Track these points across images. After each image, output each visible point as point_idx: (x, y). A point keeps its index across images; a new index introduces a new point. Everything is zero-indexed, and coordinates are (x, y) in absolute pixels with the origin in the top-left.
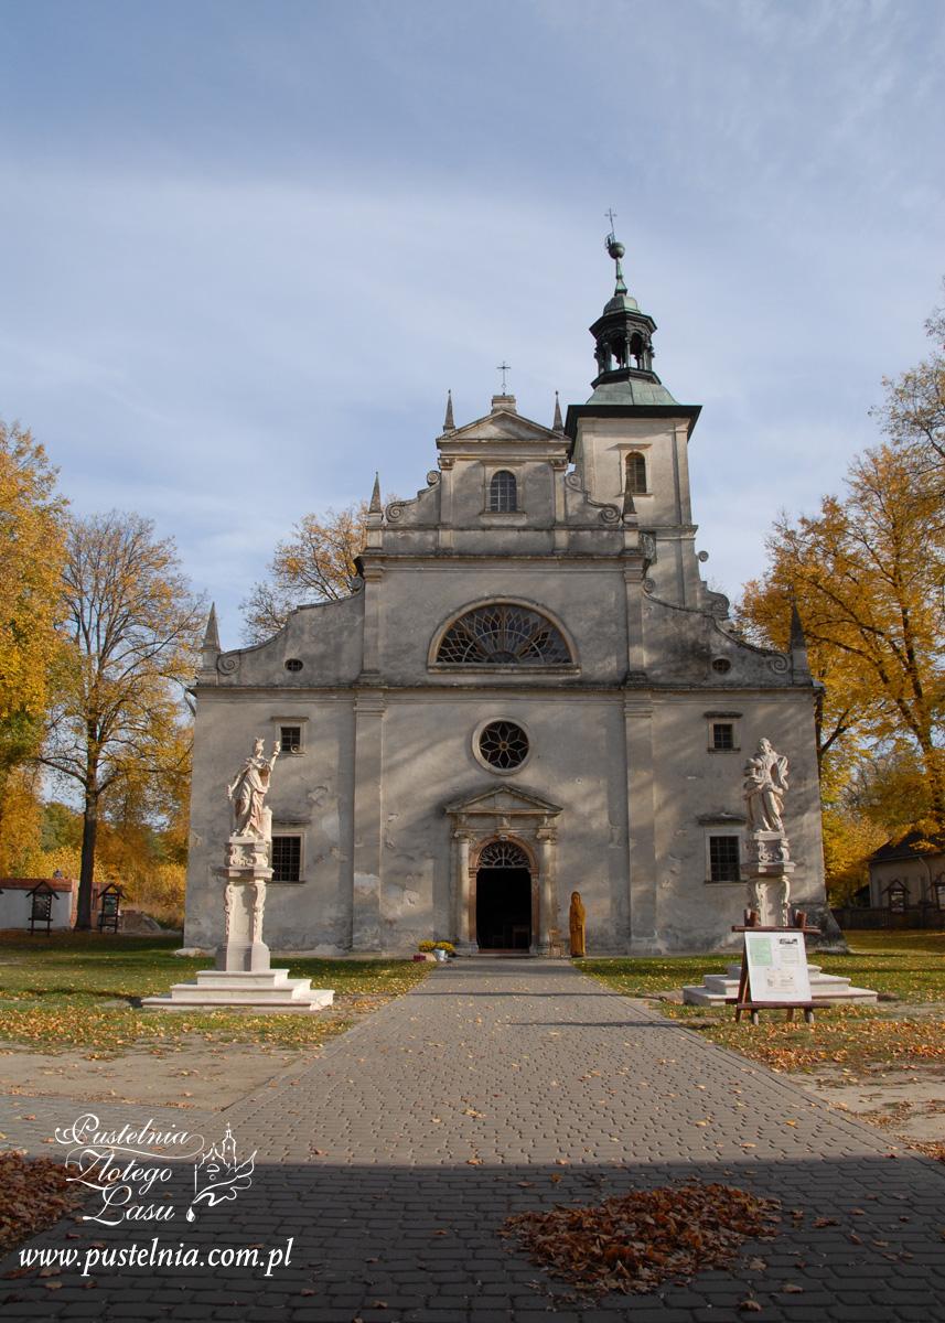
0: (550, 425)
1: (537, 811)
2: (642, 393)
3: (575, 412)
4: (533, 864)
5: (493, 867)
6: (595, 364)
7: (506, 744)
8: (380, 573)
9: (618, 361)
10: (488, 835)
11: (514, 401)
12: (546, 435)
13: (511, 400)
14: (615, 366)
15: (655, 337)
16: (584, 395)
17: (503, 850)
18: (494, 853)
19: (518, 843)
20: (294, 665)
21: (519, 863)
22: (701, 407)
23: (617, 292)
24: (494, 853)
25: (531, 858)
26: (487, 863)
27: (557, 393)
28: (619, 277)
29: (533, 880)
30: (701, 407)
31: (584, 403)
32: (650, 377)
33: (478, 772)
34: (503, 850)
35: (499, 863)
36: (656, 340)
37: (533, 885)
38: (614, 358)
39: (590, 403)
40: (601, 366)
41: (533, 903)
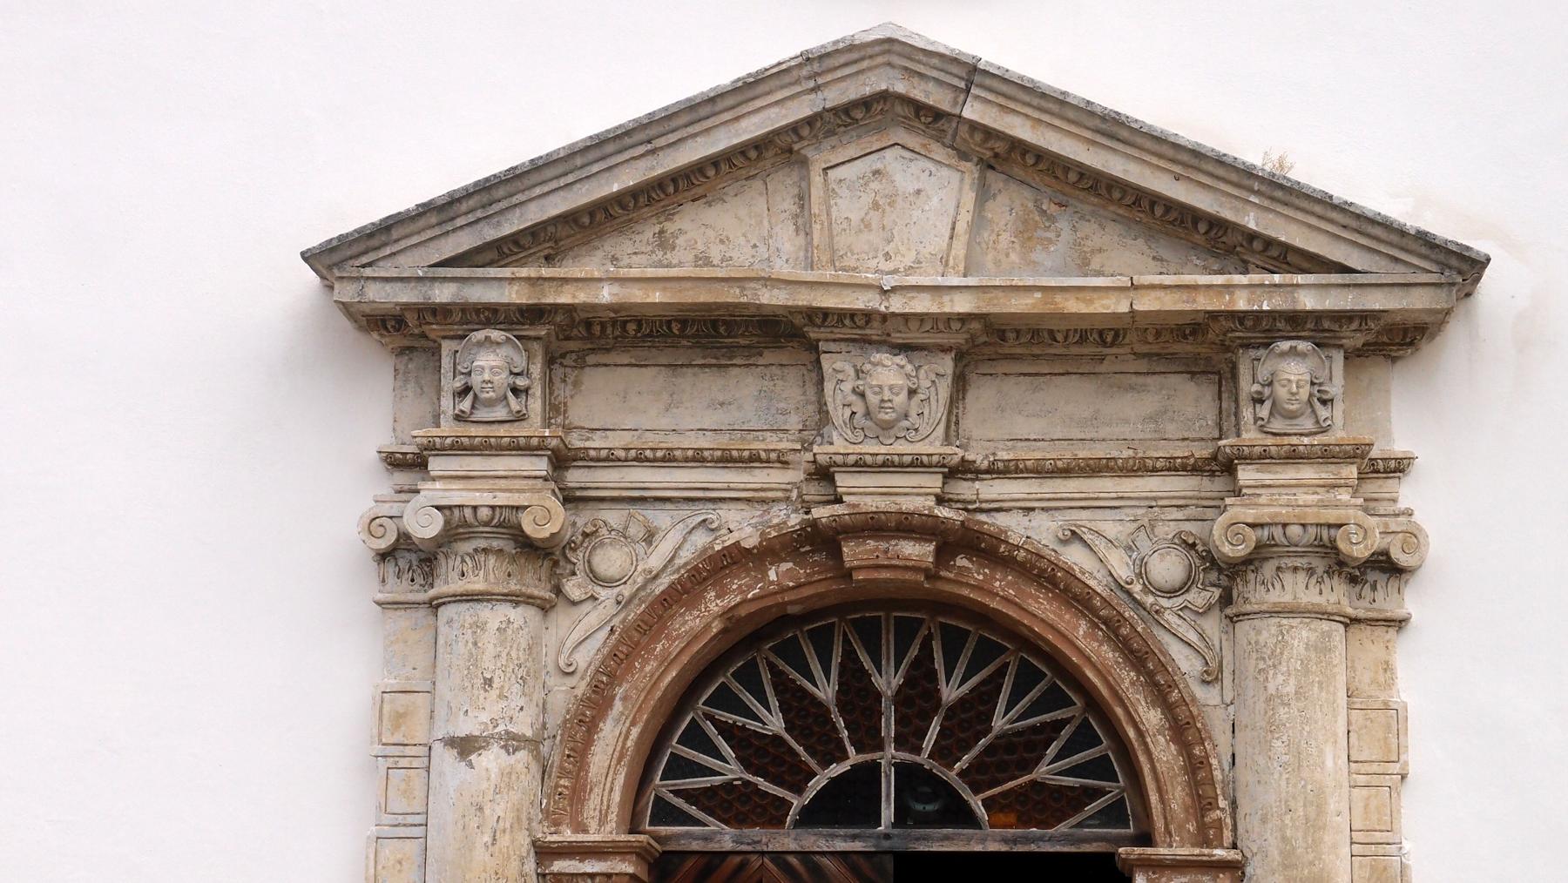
1: (1248, 291)
4: (1169, 796)
5: (787, 840)
10: (743, 528)
17: (888, 682)
18: (800, 708)
19: (1040, 610)
21: (1046, 805)
24: (800, 708)
25: (1163, 753)
26: (731, 804)
34: (888, 682)
35: (849, 802)
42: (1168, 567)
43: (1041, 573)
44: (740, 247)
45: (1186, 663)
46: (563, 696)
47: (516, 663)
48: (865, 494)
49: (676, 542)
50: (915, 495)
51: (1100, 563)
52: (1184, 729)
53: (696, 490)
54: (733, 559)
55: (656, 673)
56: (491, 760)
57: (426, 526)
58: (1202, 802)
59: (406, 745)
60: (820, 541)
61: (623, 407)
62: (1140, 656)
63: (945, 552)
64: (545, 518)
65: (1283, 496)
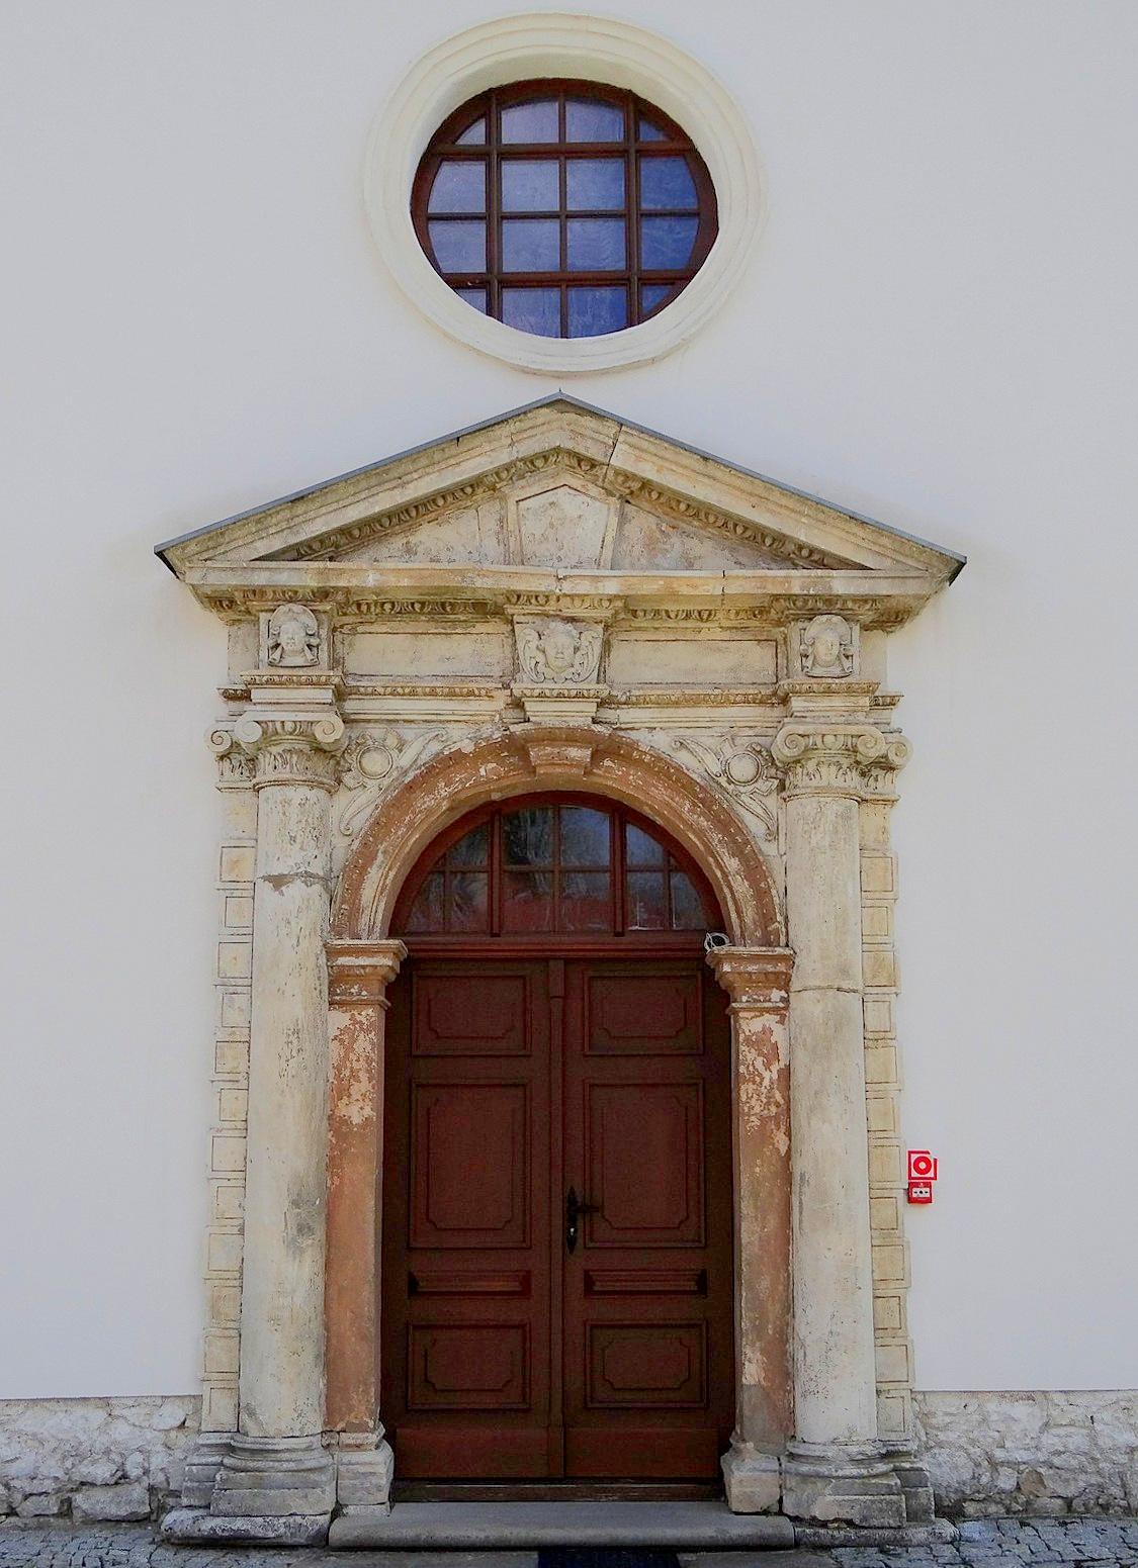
1: (798, 581)
25: (741, 887)
29: (749, 1025)
37: (747, 1058)
41: (752, 1175)
42: (743, 768)
45: (755, 827)
46: (342, 849)
48: (544, 714)
49: (419, 750)
50: (579, 714)
51: (698, 764)
52: (755, 869)
53: (438, 714)
54: (452, 761)
55: (410, 837)
56: (296, 890)
58: (766, 918)
60: (515, 748)
62: (727, 823)
63: (597, 756)
64: (329, 730)
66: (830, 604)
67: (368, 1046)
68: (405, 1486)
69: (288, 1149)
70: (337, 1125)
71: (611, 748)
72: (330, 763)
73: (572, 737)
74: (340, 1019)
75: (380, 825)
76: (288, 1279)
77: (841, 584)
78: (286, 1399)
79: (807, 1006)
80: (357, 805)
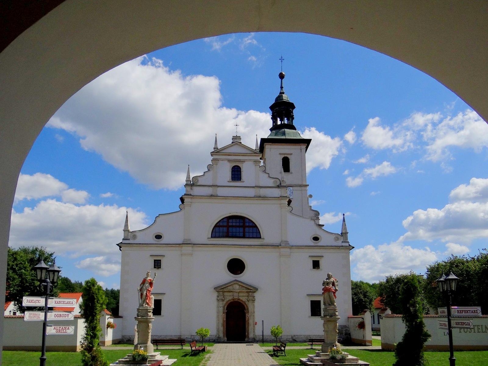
0: (254, 148)
1: (249, 291)
2: (290, 134)
3: (263, 141)
6: (271, 121)
7: (236, 266)
8: (190, 203)
9: (280, 120)
11: (240, 139)
12: (253, 152)
13: (239, 138)
14: (279, 122)
15: (294, 111)
16: (266, 134)
20: (158, 237)
22: (311, 140)
23: (281, 93)
25: (246, 307)
27: (257, 135)
28: (282, 88)
29: (247, 315)
30: (311, 140)
31: (266, 137)
32: (293, 128)
33: (228, 277)
36: (295, 112)
37: (246, 317)
38: (279, 119)
39: (270, 137)
40: (274, 122)
41: (247, 323)
42: (246, 301)
43: (242, 300)
44: (230, 288)
45: (247, 304)
47: (222, 304)
48: (235, 298)
50: (237, 298)
51: (244, 300)
52: (247, 306)
53: (229, 297)
56: (221, 308)
57: (219, 299)
58: (247, 309)
59: (218, 307)
60: (234, 299)
61: (226, 294)
62: (245, 304)
64: (223, 299)
65: (250, 298)
66: (251, 292)
67: (225, 316)
68: (227, 341)
69: (221, 321)
70: (224, 320)
71: (239, 299)
72: (223, 300)
73: (237, 299)
74: (224, 314)
75: (226, 303)
76: (221, 328)
77: (251, 291)
78: (221, 335)
79: (250, 314)
80: (225, 302)
